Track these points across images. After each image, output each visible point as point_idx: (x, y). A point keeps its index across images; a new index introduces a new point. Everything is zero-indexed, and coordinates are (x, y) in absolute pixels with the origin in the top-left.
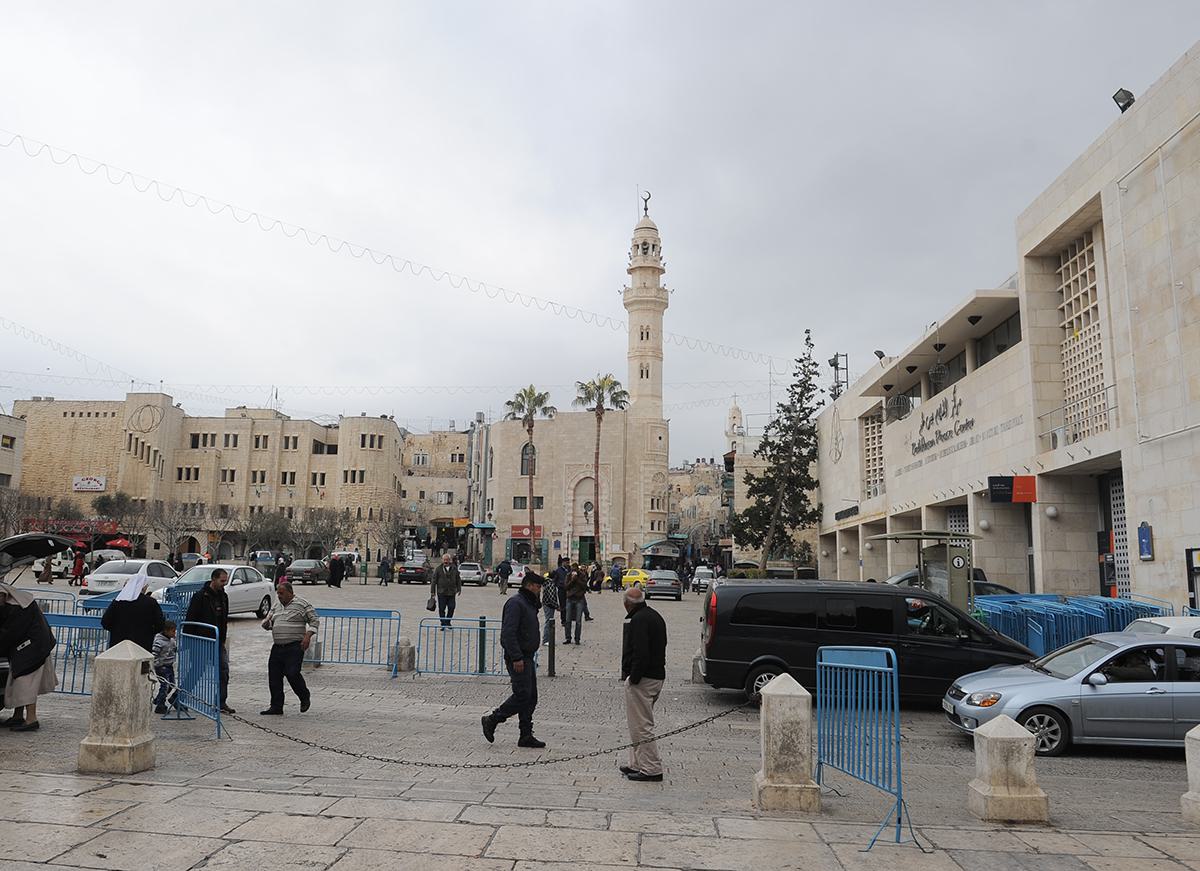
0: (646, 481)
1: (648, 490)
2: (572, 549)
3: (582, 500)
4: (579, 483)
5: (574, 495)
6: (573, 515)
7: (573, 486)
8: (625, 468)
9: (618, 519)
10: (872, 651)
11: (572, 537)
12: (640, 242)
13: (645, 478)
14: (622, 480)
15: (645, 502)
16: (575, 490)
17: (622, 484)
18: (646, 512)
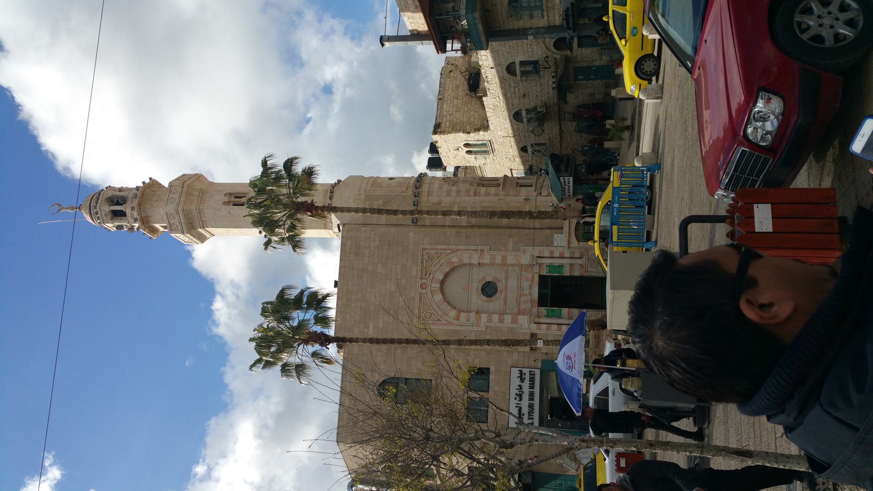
0: (453, 194)
1: (467, 192)
2: (560, 317)
3: (478, 300)
4: (448, 302)
5: (468, 311)
6: (501, 314)
7: (453, 313)
8: (432, 226)
9: (511, 236)
10: (706, 88)
11: (538, 316)
12: (107, 208)
13: (449, 193)
14: (448, 231)
15: (487, 194)
16: (460, 311)
17: (454, 230)
18: (501, 193)
